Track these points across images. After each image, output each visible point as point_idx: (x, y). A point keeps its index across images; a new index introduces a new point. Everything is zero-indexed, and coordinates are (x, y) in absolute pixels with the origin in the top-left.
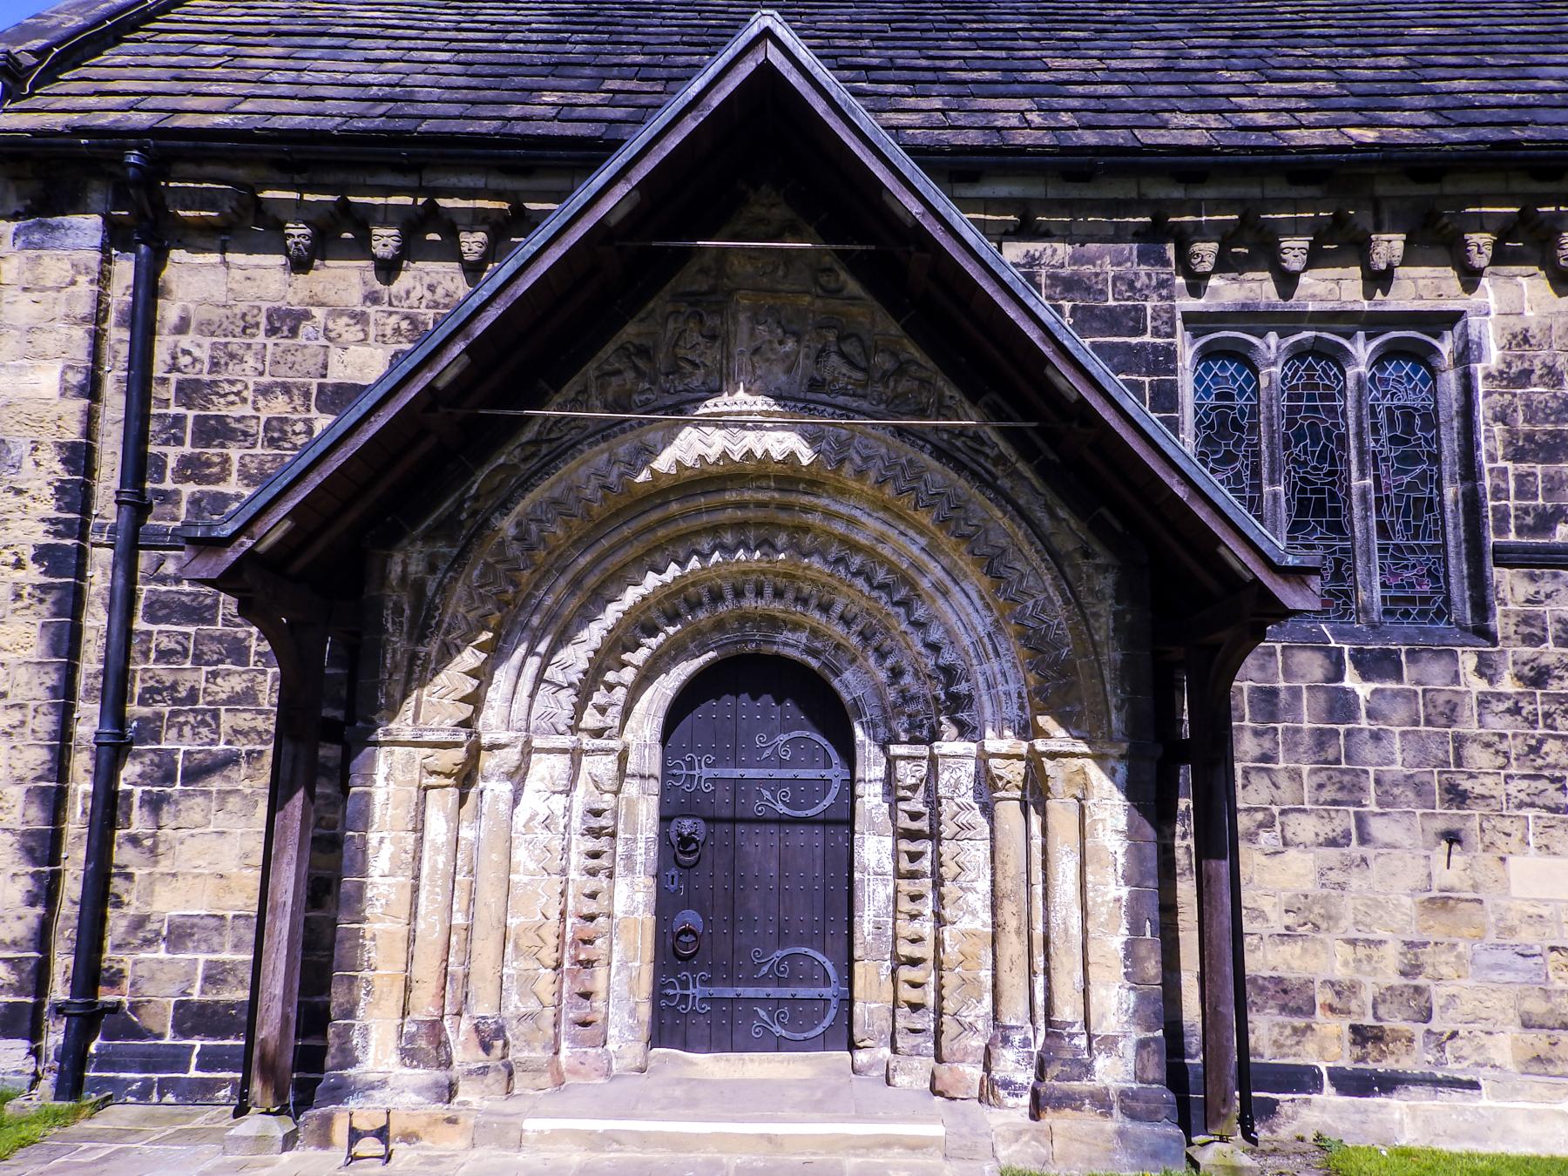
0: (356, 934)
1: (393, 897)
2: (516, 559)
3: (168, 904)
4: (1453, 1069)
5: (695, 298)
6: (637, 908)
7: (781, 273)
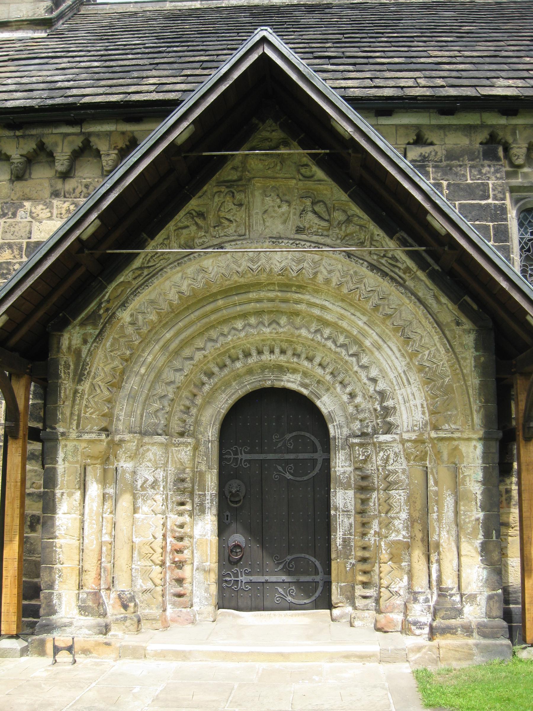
0: (52, 546)
1: (70, 525)
2: (130, 335)
5: (229, 184)
6: (207, 533)
7: (278, 168)
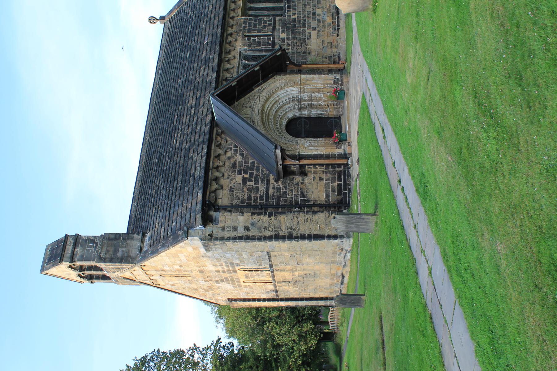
3: (323, 198)
4: (337, 55)
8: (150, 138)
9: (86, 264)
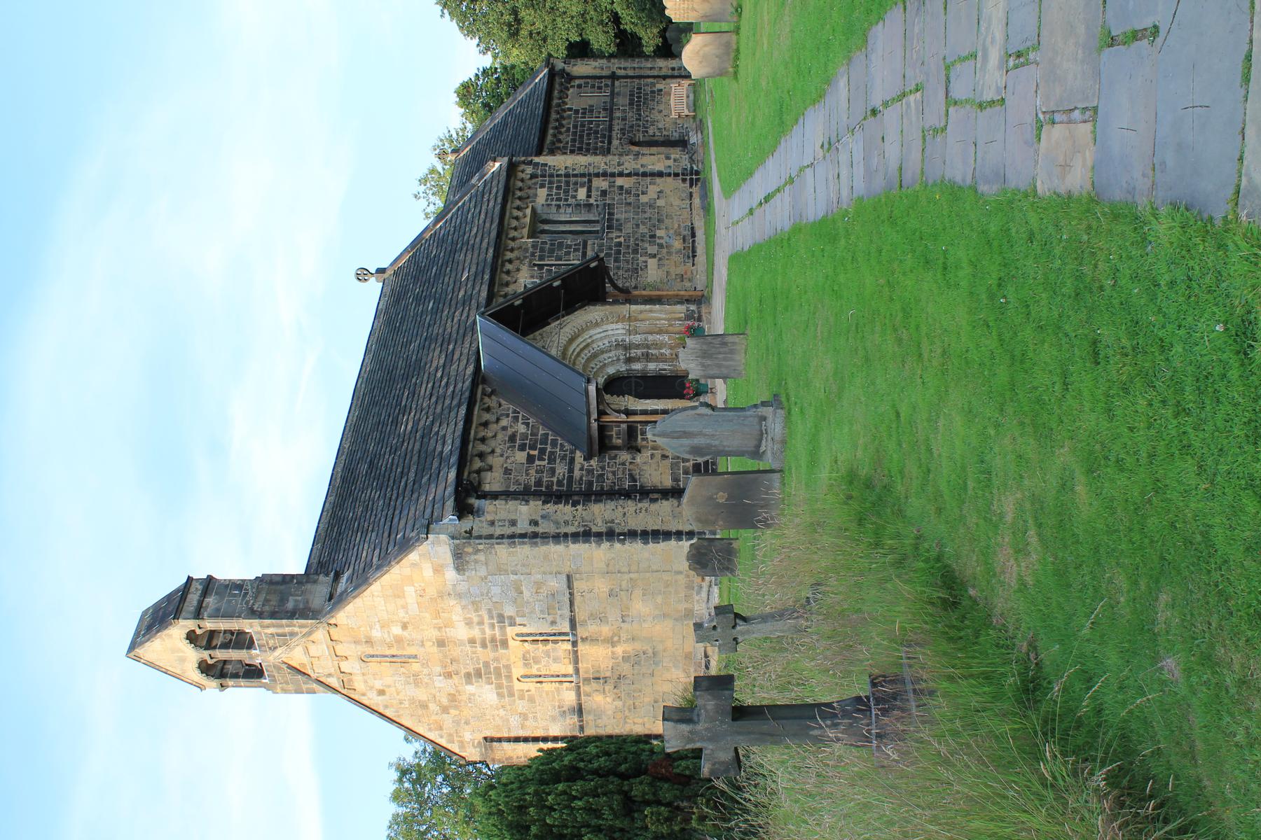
8: (352, 444)
9: (222, 625)
